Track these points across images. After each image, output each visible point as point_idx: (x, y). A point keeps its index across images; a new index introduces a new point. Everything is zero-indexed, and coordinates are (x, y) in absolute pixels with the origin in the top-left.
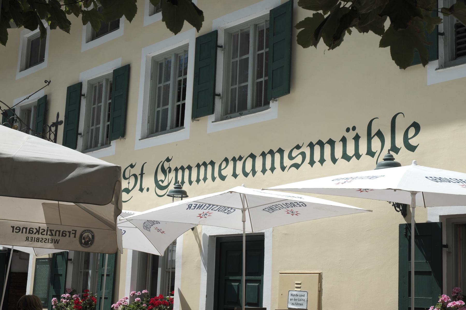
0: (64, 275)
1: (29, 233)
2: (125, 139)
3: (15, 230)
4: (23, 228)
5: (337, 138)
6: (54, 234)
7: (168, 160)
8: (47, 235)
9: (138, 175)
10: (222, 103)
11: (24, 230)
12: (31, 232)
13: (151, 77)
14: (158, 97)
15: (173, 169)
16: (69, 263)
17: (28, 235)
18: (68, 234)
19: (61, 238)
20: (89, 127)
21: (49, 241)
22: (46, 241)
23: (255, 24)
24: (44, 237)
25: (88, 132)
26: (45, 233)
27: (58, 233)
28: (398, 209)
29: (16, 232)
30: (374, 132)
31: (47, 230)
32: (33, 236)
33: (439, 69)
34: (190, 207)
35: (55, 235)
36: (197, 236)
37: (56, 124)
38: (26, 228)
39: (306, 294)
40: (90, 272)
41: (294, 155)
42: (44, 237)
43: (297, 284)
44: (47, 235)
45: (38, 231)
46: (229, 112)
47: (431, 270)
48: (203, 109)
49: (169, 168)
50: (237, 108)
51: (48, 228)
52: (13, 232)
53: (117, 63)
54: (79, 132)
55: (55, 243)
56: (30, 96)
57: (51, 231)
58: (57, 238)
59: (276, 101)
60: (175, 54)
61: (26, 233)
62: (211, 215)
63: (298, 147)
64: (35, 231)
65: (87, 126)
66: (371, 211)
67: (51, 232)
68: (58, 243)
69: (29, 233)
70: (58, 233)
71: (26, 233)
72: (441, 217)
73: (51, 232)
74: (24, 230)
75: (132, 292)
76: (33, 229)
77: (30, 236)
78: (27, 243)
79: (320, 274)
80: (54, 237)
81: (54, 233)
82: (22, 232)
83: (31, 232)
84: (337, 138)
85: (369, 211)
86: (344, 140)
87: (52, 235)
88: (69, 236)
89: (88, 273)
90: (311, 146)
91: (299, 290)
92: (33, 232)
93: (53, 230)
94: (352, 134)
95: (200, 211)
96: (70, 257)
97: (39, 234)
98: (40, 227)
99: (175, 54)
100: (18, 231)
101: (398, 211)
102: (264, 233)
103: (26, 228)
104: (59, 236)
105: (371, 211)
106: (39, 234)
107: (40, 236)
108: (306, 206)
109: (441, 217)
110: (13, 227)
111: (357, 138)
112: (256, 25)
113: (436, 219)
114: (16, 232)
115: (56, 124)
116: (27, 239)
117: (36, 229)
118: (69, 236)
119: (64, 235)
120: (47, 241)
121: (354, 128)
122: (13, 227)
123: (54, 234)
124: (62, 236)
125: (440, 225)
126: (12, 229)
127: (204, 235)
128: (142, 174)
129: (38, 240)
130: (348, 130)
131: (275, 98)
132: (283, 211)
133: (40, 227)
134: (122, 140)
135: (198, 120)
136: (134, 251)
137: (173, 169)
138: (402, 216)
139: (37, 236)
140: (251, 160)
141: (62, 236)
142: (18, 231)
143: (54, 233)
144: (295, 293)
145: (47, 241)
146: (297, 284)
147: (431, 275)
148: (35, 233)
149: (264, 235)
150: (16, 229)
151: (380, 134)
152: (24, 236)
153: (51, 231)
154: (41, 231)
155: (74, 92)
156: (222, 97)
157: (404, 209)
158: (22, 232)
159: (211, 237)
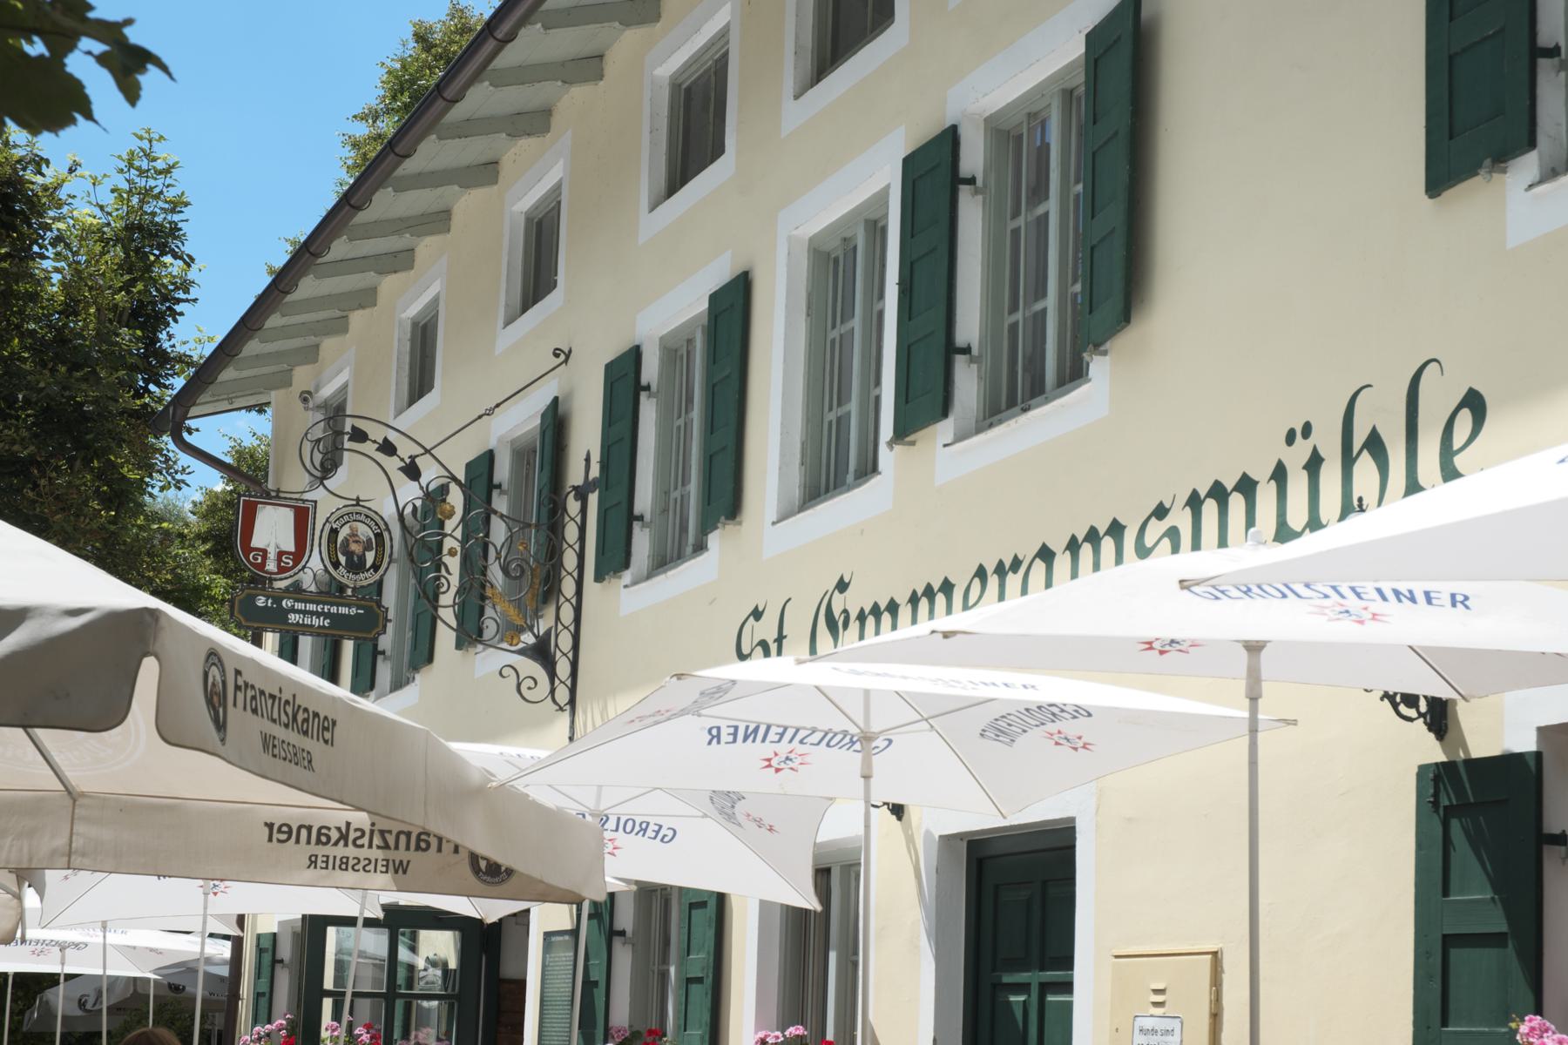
0: (602, 985)
1: (319, 842)
2: (740, 523)
3: (275, 836)
4: (300, 827)
5: (1261, 473)
6: (391, 842)
7: (842, 586)
8: (370, 846)
9: (770, 642)
10: (980, 377)
11: (304, 832)
12: (324, 839)
13: (809, 307)
14: (830, 375)
15: (854, 614)
16: (617, 943)
17: (315, 849)
18: (434, 842)
19: (412, 855)
20: (667, 493)
21: (379, 868)
22: (367, 866)
23: (1064, 91)
24: (363, 853)
25: (665, 511)
26: (365, 840)
27: (403, 838)
28: (1412, 713)
29: (279, 841)
30: (1359, 438)
31: (372, 832)
32: (329, 850)
33: (1540, 182)
34: (718, 736)
35: (397, 847)
36: (910, 840)
37: (581, 494)
38: (309, 829)
39: (1176, 1024)
40: (672, 970)
41: (1149, 541)
42: (363, 853)
43: (1156, 992)
44: (370, 846)
45: (344, 837)
46: (1004, 405)
47: (1504, 928)
48: (925, 400)
49: (845, 611)
50: (1020, 387)
51: (373, 824)
52: (270, 840)
53: (717, 275)
54: (637, 510)
55: (396, 872)
56: (498, 406)
57: (382, 832)
58: (401, 855)
59: (1105, 353)
60: (867, 221)
61: (309, 842)
62: (807, 759)
63: (1161, 512)
64: (335, 835)
65: (663, 492)
66: (1295, 722)
67: (385, 838)
68: (405, 872)
69: (319, 842)
70: (403, 838)
71: (309, 842)
72: (1543, 732)
73: (385, 838)
74: (304, 832)
75: (761, 1034)
76: (428, 835)
77: (321, 851)
78: (311, 873)
79: (1215, 954)
80: (391, 854)
81: (391, 839)
82: (298, 841)
83: (324, 839)
84: (1261, 473)
85: (1287, 722)
86: (1280, 474)
87: (386, 847)
88: (439, 850)
89: (664, 976)
90: (1195, 502)
91: (1159, 1011)
92: (329, 838)
93: (390, 832)
94: (1302, 449)
95: (767, 749)
96: (618, 926)
97: (346, 845)
98: (348, 824)
99: (867, 221)
100: (284, 837)
101: (1410, 720)
102: (1073, 820)
103: (309, 829)
104: (408, 848)
105: (1295, 722)
106: (346, 845)
107: (351, 851)
108: (1090, 715)
109: (1543, 732)
110: (270, 826)
111: (1314, 464)
112: (1071, 92)
113: (1525, 743)
114: (279, 841)
115: (581, 494)
116: (313, 862)
117: (339, 829)
118: (439, 850)
119: (423, 845)
120: (371, 867)
121: (1307, 430)
122: (270, 826)
123: (391, 842)
124: (418, 848)
125: (1532, 764)
126: (266, 830)
127: (928, 834)
128: (780, 639)
129: (344, 864)
130: (1290, 438)
131: (1097, 346)
132: (1036, 734)
133: (348, 824)
134: (730, 528)
135: (913, 443)
136: (763, 903)
137: (854, 614)
138: (1432, 736)
139: (340, 851)
140: (1043, 565)
141: (418, 848)
142: (284, 837)
143: (391, 839)
144: (1148, 1023)
145: (371, 867)
146: (1156, 992)
147: (1505, 946)
148: (336, 844)
149: (1073, 828)
150: (279, 831)
151: (1375, 444)
152: (304, 850)
153: (382, 832)
154: (352, 835)
155: (624, 378)
156: (980, 356)
157: (1439, 716)
158: (298, 841)
159: (947, 840)
